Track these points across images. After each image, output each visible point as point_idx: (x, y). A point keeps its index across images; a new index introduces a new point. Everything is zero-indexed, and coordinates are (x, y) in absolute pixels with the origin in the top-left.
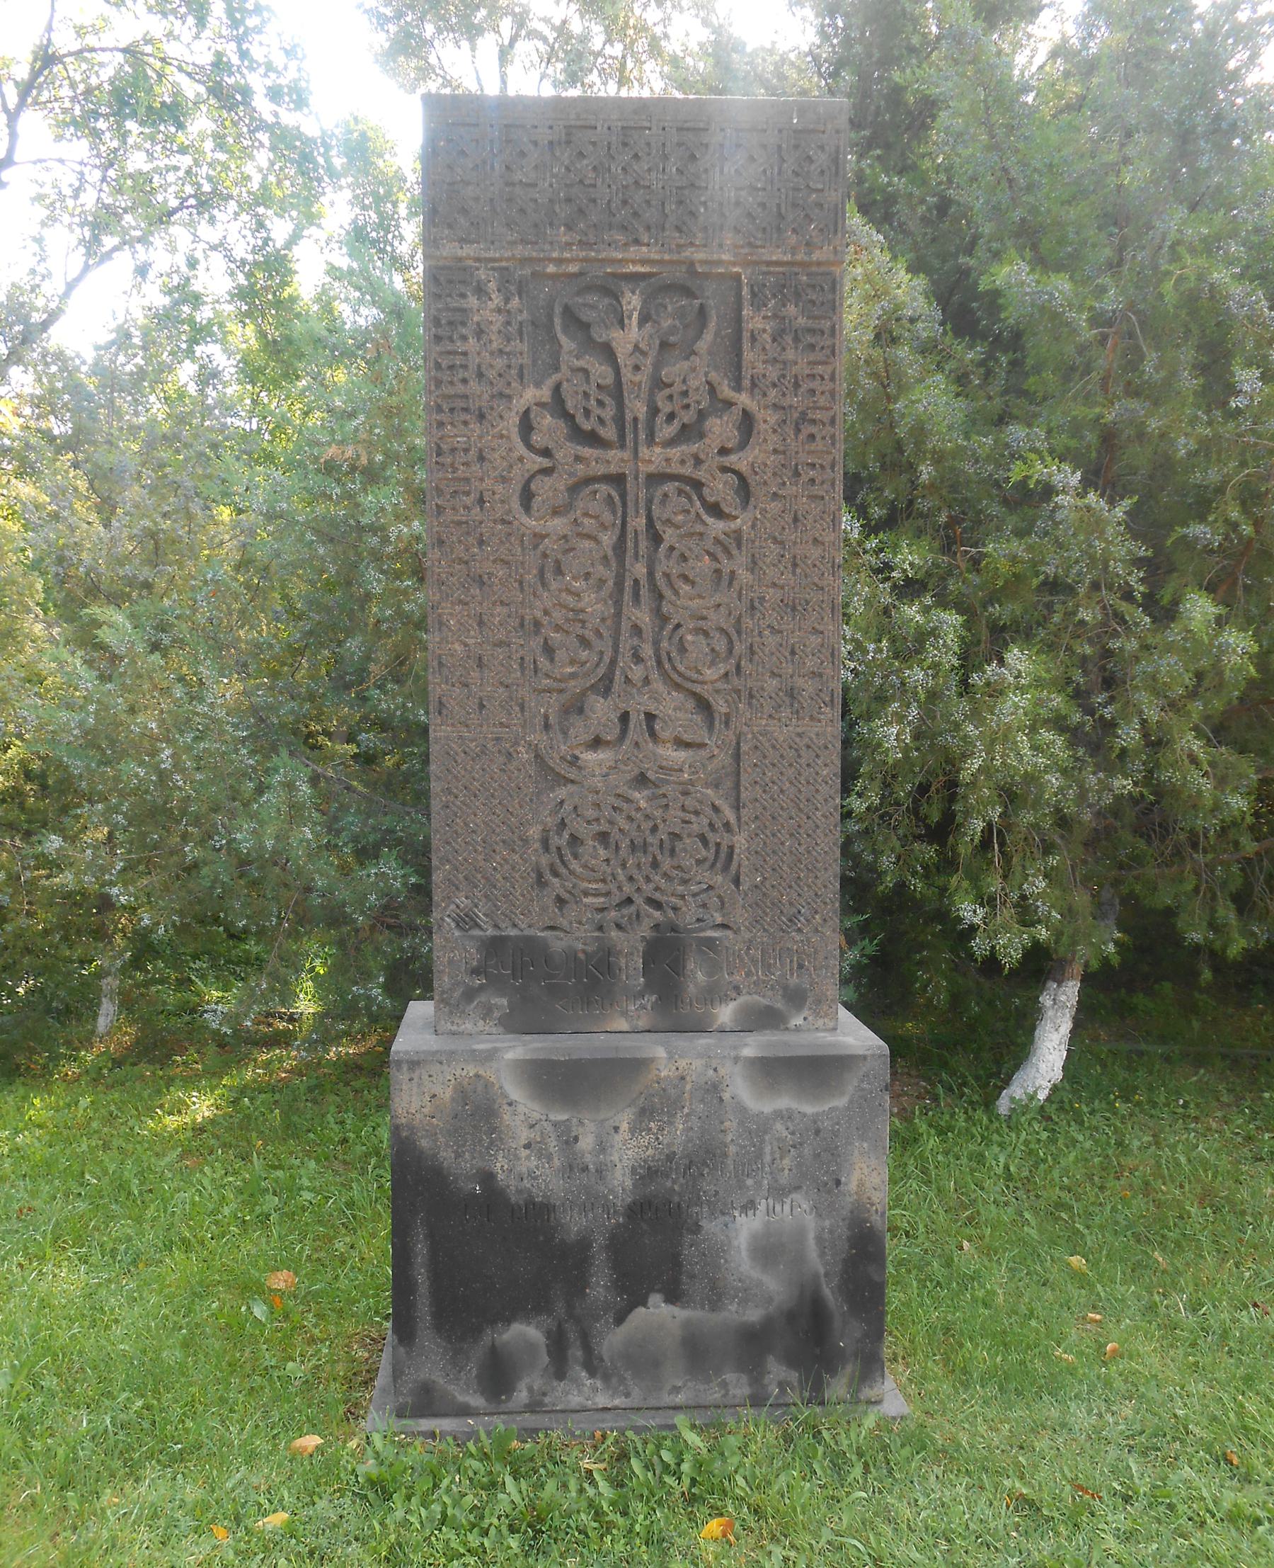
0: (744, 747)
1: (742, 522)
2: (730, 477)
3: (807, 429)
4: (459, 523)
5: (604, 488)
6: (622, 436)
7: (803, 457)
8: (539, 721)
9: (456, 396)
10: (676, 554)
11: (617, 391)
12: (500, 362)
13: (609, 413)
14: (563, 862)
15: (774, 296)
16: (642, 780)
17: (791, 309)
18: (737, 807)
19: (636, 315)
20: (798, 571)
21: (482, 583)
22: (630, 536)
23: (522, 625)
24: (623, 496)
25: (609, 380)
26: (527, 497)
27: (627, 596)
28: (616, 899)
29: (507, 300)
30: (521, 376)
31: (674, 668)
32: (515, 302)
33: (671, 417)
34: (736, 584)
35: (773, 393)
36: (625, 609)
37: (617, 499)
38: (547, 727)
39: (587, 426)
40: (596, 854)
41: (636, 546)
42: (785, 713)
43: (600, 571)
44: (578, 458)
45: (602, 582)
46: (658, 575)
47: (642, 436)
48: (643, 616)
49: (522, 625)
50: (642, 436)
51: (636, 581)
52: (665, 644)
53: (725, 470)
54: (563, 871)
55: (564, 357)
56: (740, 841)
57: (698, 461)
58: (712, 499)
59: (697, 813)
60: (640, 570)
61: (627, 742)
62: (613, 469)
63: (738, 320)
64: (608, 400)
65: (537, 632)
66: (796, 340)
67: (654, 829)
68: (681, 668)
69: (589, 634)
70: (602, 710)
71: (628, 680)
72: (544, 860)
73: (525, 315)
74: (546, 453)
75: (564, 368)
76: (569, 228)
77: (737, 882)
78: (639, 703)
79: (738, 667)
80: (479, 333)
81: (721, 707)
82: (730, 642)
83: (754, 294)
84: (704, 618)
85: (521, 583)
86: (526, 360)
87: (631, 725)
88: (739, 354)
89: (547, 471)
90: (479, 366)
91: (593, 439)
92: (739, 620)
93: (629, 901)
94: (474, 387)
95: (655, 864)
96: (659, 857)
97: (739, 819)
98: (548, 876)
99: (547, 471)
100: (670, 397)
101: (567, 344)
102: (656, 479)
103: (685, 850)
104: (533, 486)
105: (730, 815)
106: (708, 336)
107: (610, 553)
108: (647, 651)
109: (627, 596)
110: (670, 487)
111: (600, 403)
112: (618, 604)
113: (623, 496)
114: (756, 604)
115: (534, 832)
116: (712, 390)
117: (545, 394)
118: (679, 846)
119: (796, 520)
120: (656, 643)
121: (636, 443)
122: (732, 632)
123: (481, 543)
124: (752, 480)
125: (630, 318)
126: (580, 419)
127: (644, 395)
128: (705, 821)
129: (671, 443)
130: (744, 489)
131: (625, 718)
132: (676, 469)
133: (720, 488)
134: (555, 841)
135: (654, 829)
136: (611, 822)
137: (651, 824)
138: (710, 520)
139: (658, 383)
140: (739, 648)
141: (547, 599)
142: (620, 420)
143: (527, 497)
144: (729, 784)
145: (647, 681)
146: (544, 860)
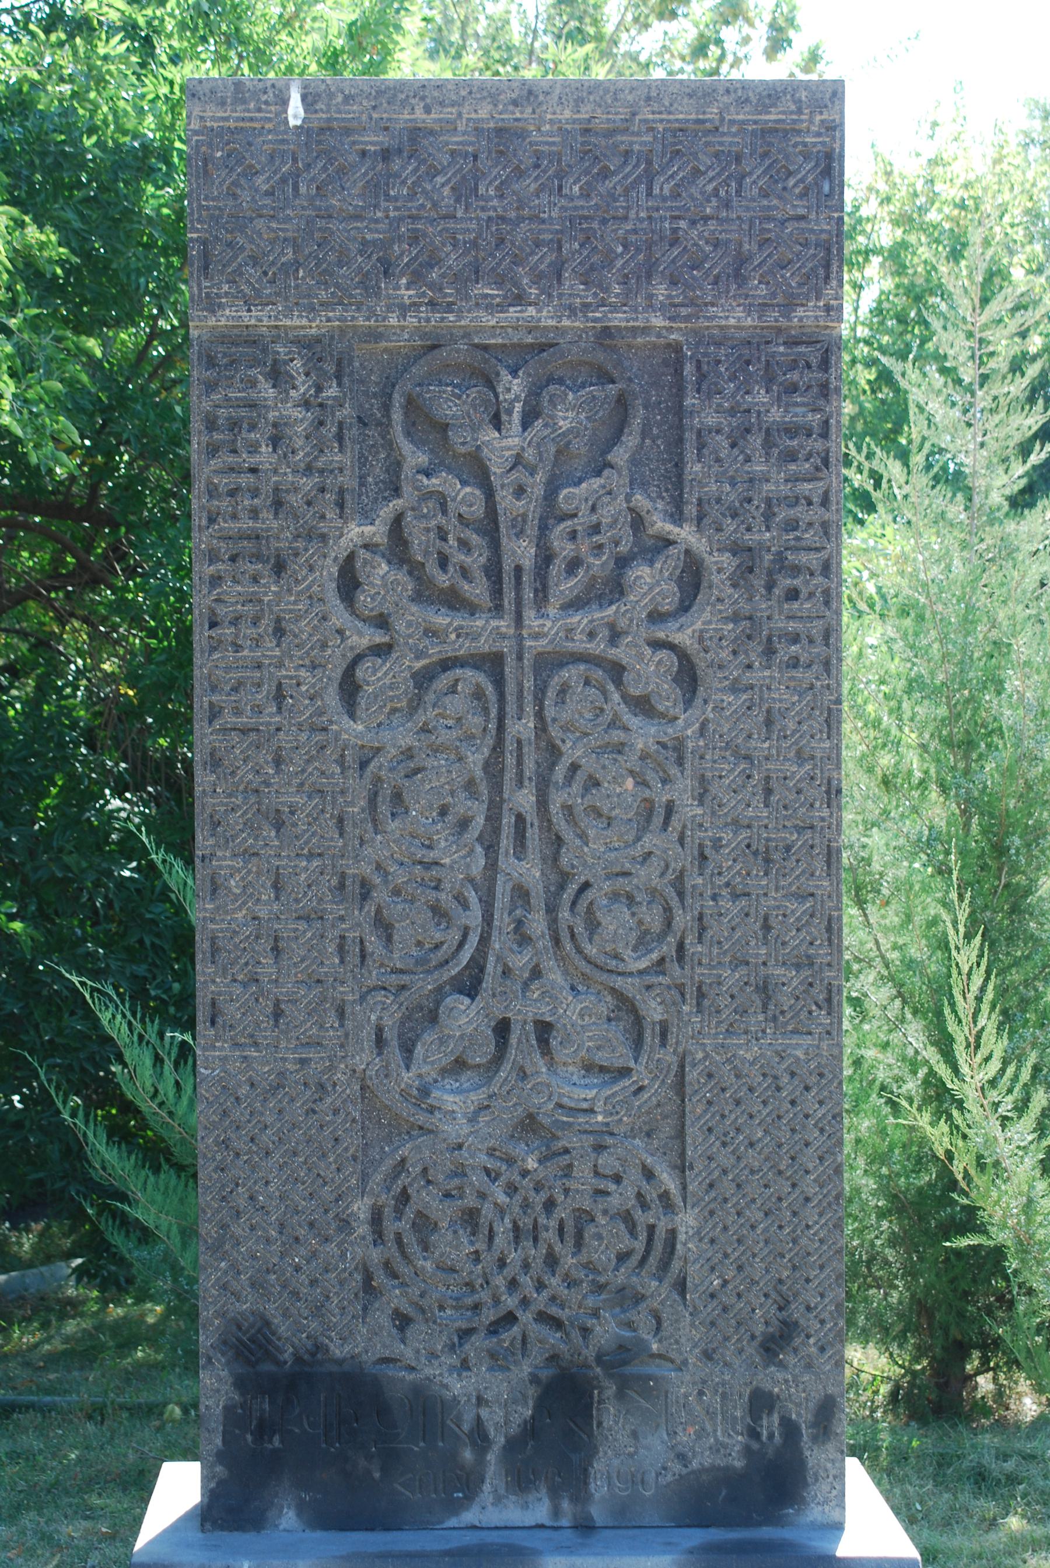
0: (692, 1075)
1: (686, 725)
2: (663, 654)
3: (786, 582)
4: (244, 731)
5: (470, 675)
6: (497, 592)
7: (780, 623)
8: (367, 1034)
9: (242, 536)
10: (580, 777)
11: (490, 526)
12: (307, 484)
13: (477, 560)
14: (404, 1255)
15: (733, 378)
16: (529, 1125)
17: (761, 396)
18: (682, 1168)
19: (518, 407)
20: (774, 798)
21: (279, 826)
22: (510, 746)
23: (342, 886)
24: (499, 683)
25: (478, 510)
26: (350, 689)
27: (506, 842)
28: (489, 1315)
29: (319, 389)
30: (341, 505)
31: (579, 951)
32: (332, 391)
33: (573, 565)
34: (675, 823)
35: (730, 525)
36: (502, 864)
37: (490, 689)
38: (380, 1042)
39: (443, 580)
40: (454, 1246)
41: (520, 762)
42: (756, 1019)
43: (463, 805)
44: (431, 632)
45: (464, 824)
46: (555, 808)
47: (528, 595)
48: (530, 871)
49: (342, 886)
50: (528, 595)
51: (520, 818)
52: (564, 914)
53: (657, 645)
54: (403, 1269)
55: (407, 471)
56: (687, 1221)
57: (615, 636)
58: (635, 691)
59: (617, 1179)
60: (525, 799)
61: (507, 1066)
62: (484, 645)
63: (679, 411)
64: (475, 539)
65: (365, 896)
66: (768, 444)
67: (550, 1205)
68: (591, 950)
69: (445, 898)
70: (465, 1017)
71: (506, 972)
72: (376, 1255)
73: (347, 412)
74: (382, 622)
75: (406, 489)
76: (417, 279)
77: (681, 1287)
78: (524, 1011)
79: (681, 947)
80: (275, 441)
81: (654, 1011)
82: (668, 909)
83: (702, 377)
84: (626, 874)
85: (341, 821)
86: (347, 480)
87: (513, 1040)
88: (679, 466)
89: (382, 651)
90: (276, 490)
91: (453, 601)
92: (681, 876)
93: (510, 1318)
94: (269, 522)
95: (552, 1261)
96: (558, 1248)
97: (684, 1187)
98: (380, 1279)
99: (382, 651)
100: (573, 536)
101: (414, 457)
102: (548, 664)
103: (599, 1237)
104: (359, 673)
105: (668, 1181)
106: (631, 440)
107: (479, 773)
108: (537, 924)
109: (506, 842)
110: (571, 674)
111: (464, 545)
112: (491, 849)
113: (499, 683)
114: (708, 852)
115: (361, 1208)
116: (638, 522)
117: (376, 531)
118: (590, 1230)
119: (769, 723)
120: (551, 910)
121: (519, 602)
122: (671, 893)
123: (278, 762)
124: (701, 662)
125: (510, 412)
126: (432, 568)
127: (532, 529)
128: (631, 1192)
129: (575, 604)
130: (688, 677)
131: (503, 1029)
132: (580, 644)
133: (651, 673)
134: (391, 1227)
135: (550, 1205)
136: (482, 1196)
137: (543, 1196)
138: (635, 722)
139: (551, 514)
140: (682, 919)
141: (378, 848)
142: (494, 571)
143: (350, 689)
144: (667, 1129)
145: (536, 973)
146: (376, 1255)
